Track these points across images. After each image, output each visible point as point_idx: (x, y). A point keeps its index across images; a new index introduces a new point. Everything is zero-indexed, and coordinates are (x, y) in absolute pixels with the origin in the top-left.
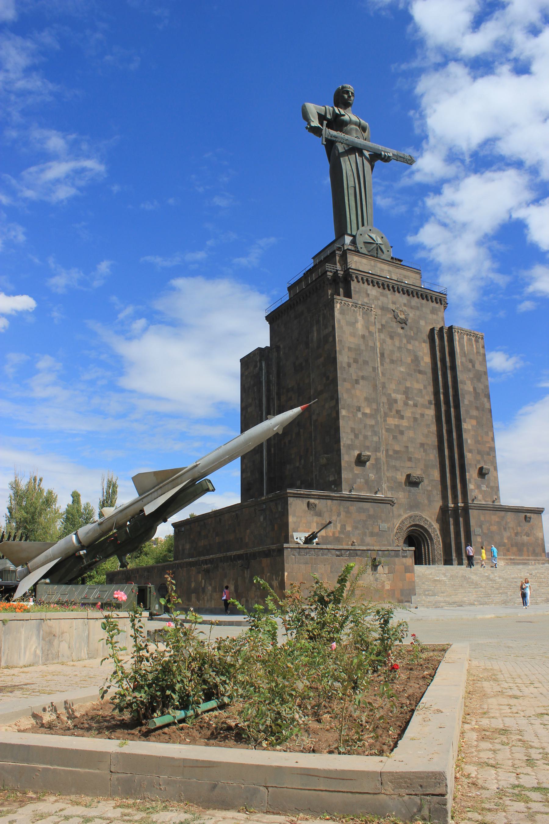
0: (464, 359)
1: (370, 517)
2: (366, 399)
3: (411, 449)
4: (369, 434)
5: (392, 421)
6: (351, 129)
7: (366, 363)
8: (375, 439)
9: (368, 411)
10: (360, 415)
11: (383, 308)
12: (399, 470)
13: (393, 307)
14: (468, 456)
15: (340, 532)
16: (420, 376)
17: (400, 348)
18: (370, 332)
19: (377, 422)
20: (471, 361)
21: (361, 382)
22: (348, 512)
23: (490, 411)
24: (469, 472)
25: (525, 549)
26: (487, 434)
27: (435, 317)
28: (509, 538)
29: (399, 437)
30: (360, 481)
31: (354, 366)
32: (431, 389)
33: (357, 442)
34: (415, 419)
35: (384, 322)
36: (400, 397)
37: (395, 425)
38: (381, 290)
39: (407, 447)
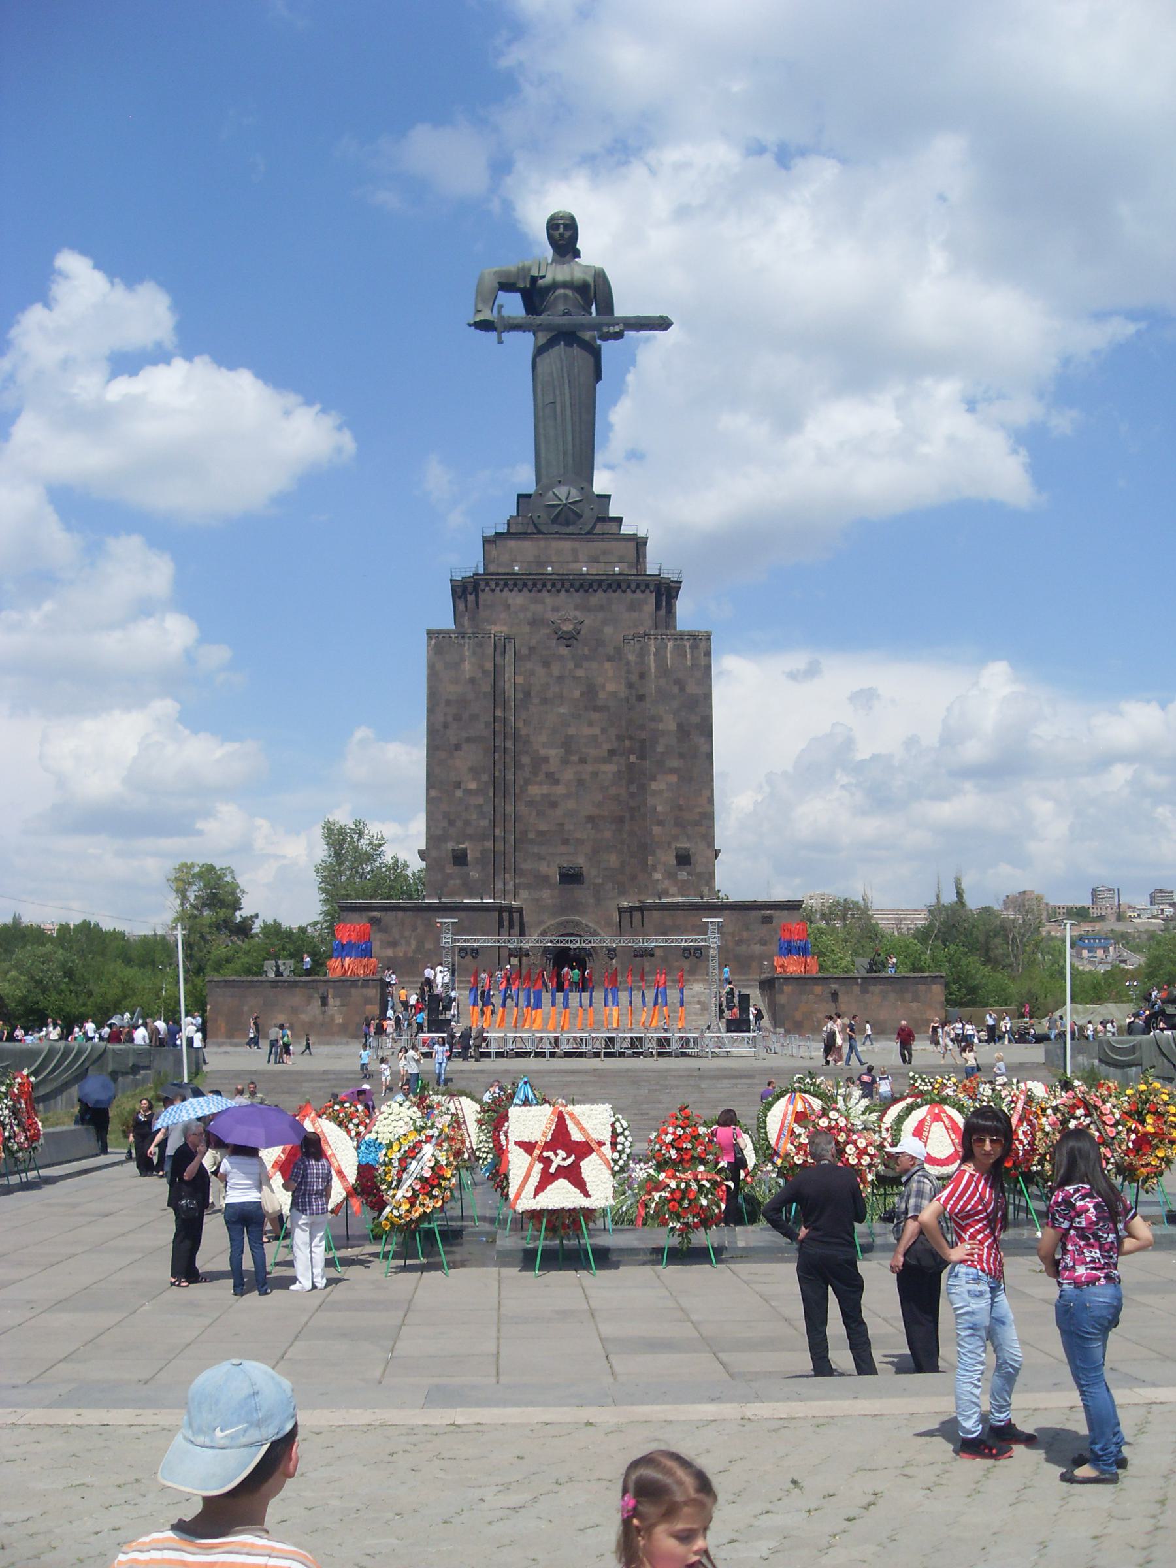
0: (663, 682)
2: (472, 769)
3: (567, 828)
4: (474, 817)
5: (535, 791)
6: (557, 298)
7: (474, 718)
8: (484, 823)
9: (473, 786)
10: (459, 793)
11: (534, 623)
12: (544, 859)
13: (554, 617)
14: (656, 830)
15: (415, 952)
16: (595, 716)
17: (561, 678)
18: (485, 672)
21: (465, 747)
23: (710, 756)
24: (653, 853)
25: (754, 964)
27: (635, 615)
30: (455, 883)
32: (613, 732)
34: (580, 783)
35: (533, 643)
36: (554, 753)
37: (542, 795)
38: (532, 594)
39: (562, 825)
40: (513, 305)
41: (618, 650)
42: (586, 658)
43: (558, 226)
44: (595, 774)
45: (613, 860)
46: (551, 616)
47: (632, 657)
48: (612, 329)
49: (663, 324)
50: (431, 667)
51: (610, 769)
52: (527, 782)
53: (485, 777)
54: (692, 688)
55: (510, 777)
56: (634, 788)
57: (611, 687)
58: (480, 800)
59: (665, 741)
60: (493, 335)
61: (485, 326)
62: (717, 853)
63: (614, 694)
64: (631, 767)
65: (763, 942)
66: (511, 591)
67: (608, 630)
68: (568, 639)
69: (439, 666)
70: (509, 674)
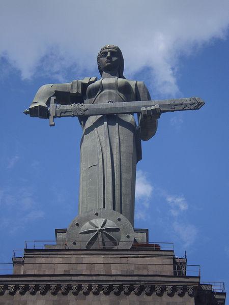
38: (56, 298)
43: (106, 53)
48: (149, 108)
66: (33, 294)
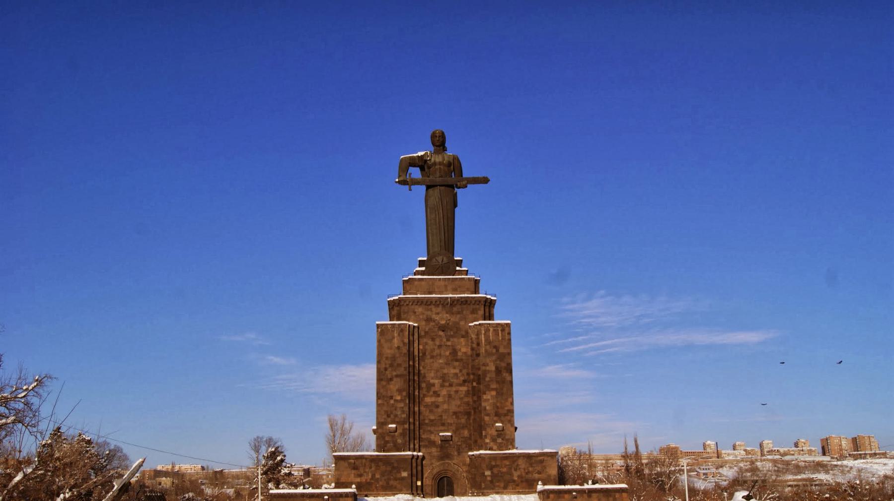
0: (488, 347)
1: (393, 468)
4: (399, 413)
5: (428, 400)
7: (399, 365)
8: (404, 416)
9: (399, 398)
10: (392, 402)
14: (487, 418)
16: (457, 364)
17: (440, 346)
18: (404, 344)
19: (405, 404)
20: (495, 347)
22: (377, 466)
23: (511, 382)
24: (485, 430)
26: (506, 400)
28: (518, 476)
29: (435, 410)
31: (390, 369)
32: (465, 371)
33: (389, 420)
34: (450, 396)
40: (415, 173)
41: (467, 332)
42: (452, 336)
44: (457, 392)
45: (466, 433)
46: (434, 316)
47: (474, 336)
49: (485, 181)
50: (379, 341)
51: (464, 389)
52: (425, 396)
53: (404, 394)
54: (502, 350)
55: (417, 393)
56: (475, 398)
57: (464, 350)
58: (402, 405)
59: (489, 377)
60: (407, 187)
61: (403, 182)
62: (516, 428)
63: (465, 353)
64: (473, 388)
65: (539, 473)
67: (462, 323)
68: (443, 328)
69: (383, 341)
70: (416, 345)
